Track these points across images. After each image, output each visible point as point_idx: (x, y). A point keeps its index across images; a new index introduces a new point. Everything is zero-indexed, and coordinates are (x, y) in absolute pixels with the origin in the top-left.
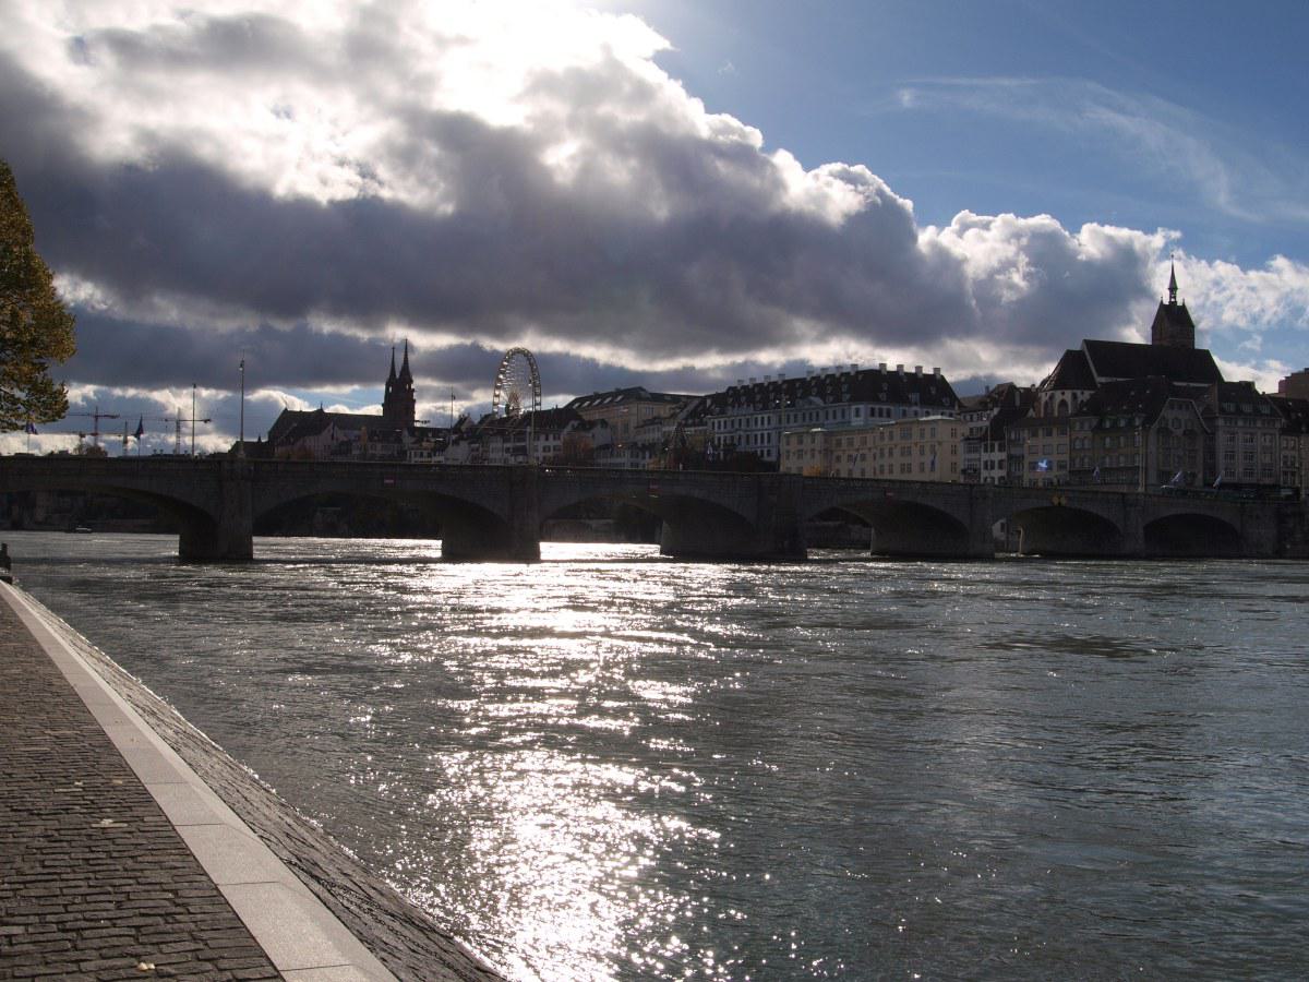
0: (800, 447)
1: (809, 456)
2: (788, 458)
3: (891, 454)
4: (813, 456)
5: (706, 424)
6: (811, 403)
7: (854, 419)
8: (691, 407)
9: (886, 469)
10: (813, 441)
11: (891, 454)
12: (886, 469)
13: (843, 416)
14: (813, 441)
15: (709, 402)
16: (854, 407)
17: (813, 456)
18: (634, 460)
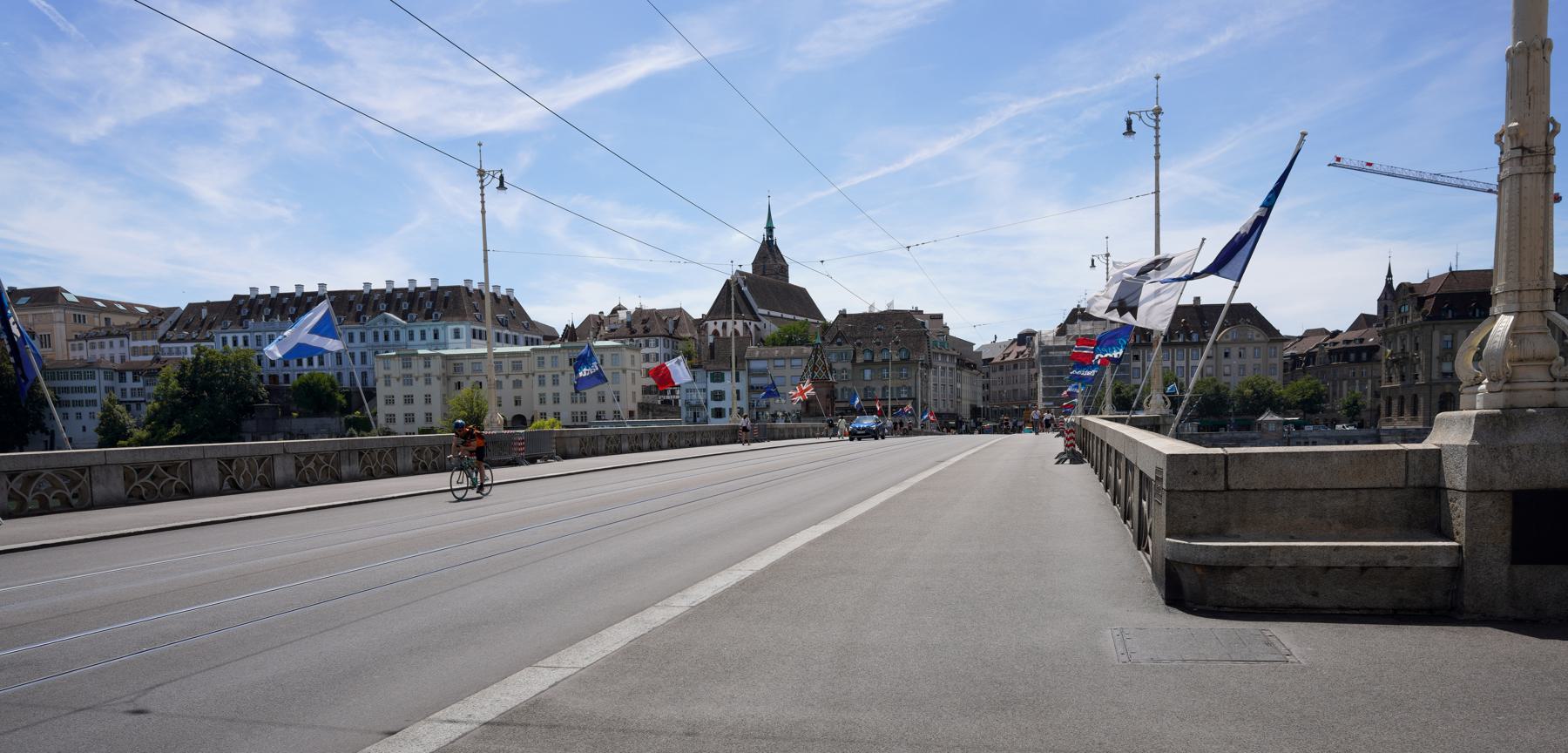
0: (408, 371)
1: (422, 380)
2: (388, 384)
3: (556, 382)
4: (428, 382)
5: (210, 339)
6: (386, 320)
7: (451, 340)
8: (173, 318)
9: (549, 399)
10: (427, 365)
11: (556, 382)
12: (549, 399)
13: (436, 336)
14: (427, 365)
15: (204, 312)
16: (451, 328)
17: (428, 382)
18: (109, 383)
